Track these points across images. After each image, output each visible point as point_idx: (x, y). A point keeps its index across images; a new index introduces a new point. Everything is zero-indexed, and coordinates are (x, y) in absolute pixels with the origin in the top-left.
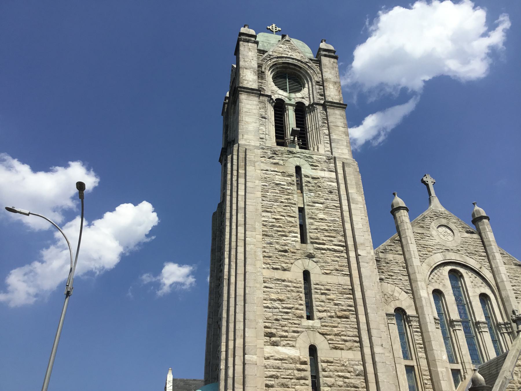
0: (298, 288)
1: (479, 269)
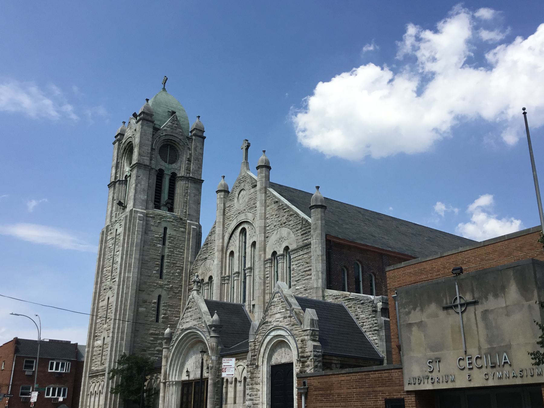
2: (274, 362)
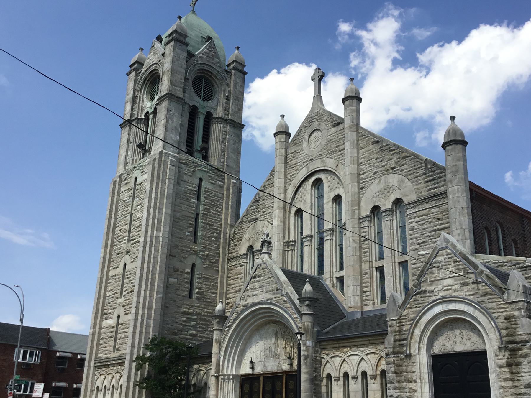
1: (336, 169)
2: (438, 350)
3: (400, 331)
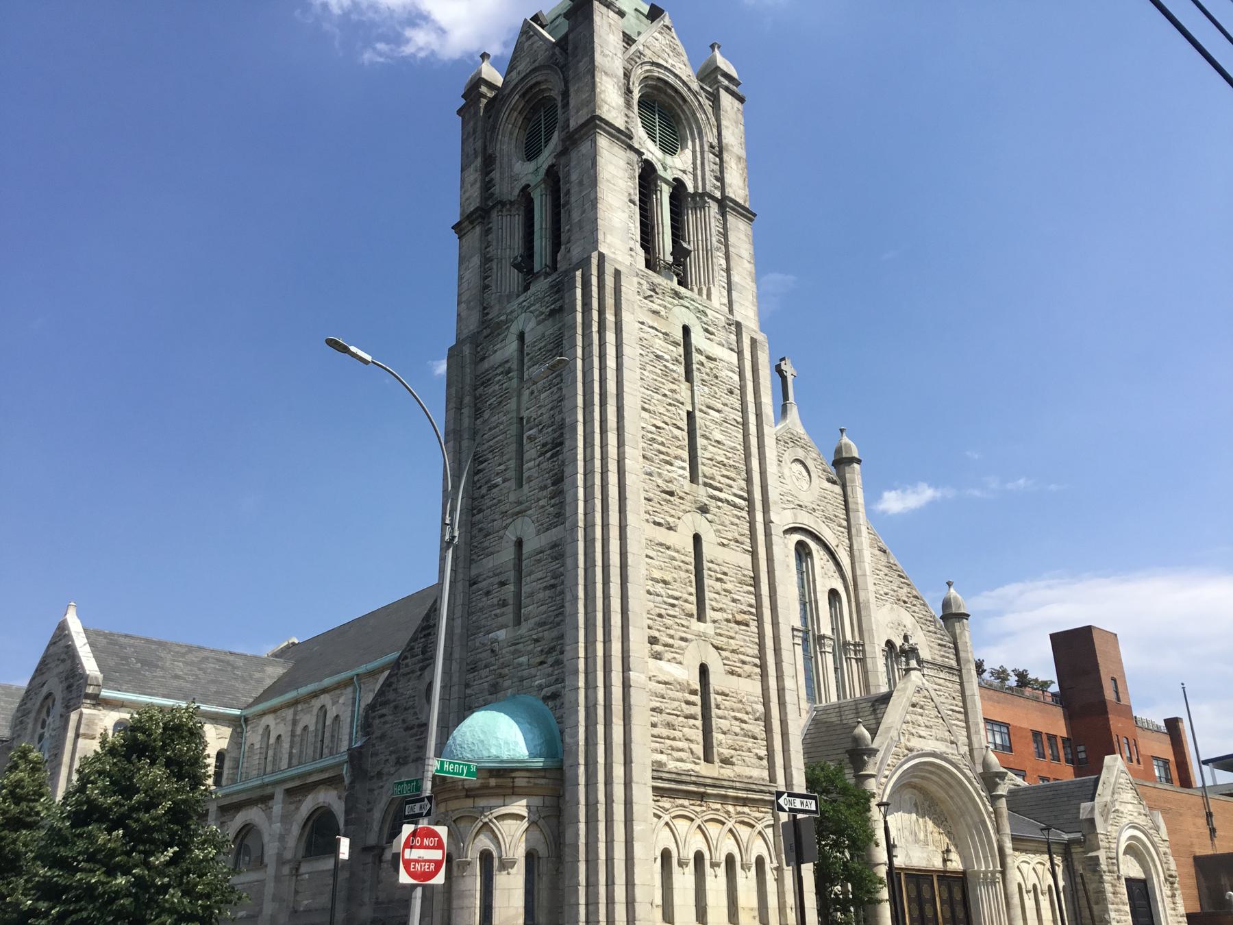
0: (687, 564)
3: (1109, 848)
